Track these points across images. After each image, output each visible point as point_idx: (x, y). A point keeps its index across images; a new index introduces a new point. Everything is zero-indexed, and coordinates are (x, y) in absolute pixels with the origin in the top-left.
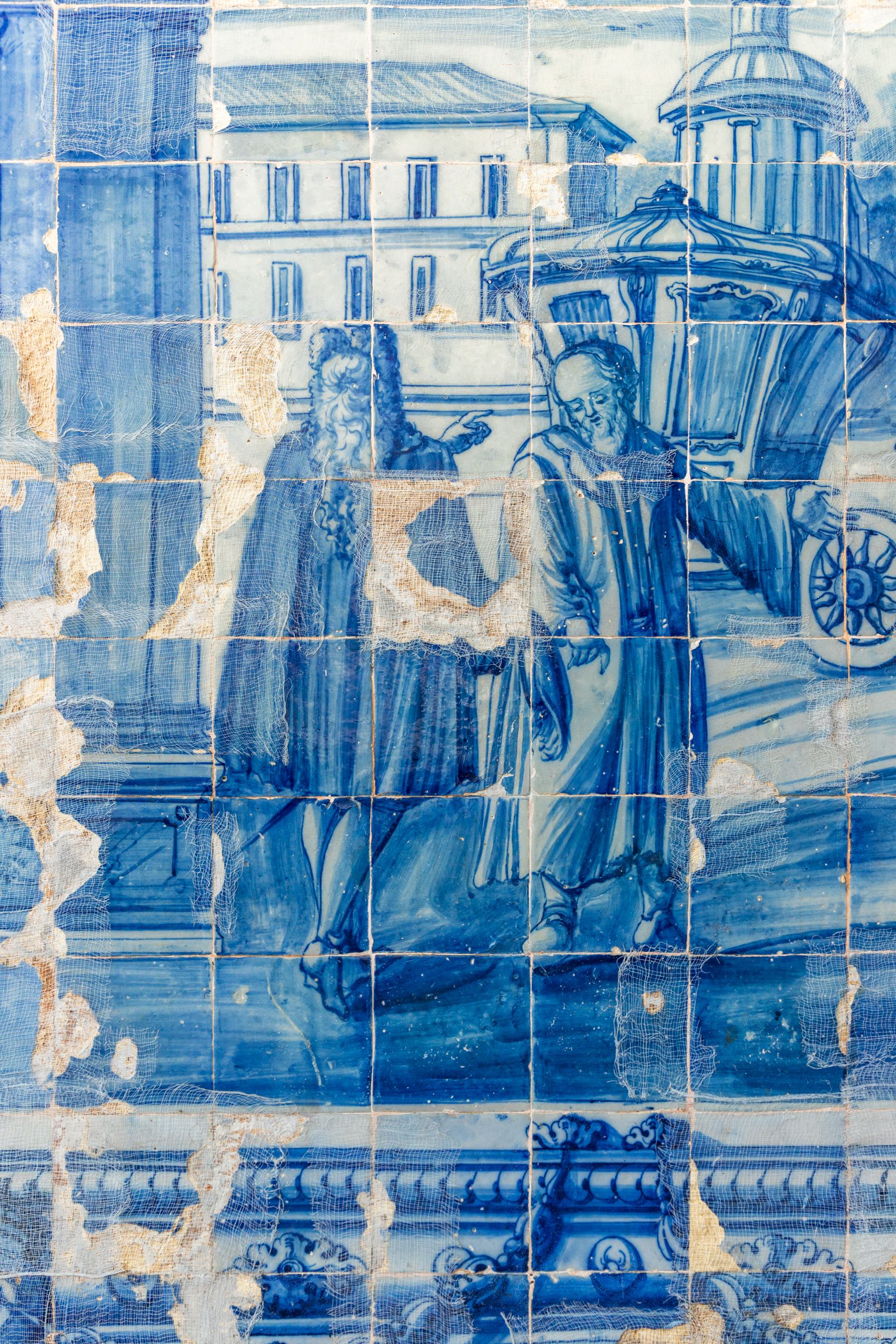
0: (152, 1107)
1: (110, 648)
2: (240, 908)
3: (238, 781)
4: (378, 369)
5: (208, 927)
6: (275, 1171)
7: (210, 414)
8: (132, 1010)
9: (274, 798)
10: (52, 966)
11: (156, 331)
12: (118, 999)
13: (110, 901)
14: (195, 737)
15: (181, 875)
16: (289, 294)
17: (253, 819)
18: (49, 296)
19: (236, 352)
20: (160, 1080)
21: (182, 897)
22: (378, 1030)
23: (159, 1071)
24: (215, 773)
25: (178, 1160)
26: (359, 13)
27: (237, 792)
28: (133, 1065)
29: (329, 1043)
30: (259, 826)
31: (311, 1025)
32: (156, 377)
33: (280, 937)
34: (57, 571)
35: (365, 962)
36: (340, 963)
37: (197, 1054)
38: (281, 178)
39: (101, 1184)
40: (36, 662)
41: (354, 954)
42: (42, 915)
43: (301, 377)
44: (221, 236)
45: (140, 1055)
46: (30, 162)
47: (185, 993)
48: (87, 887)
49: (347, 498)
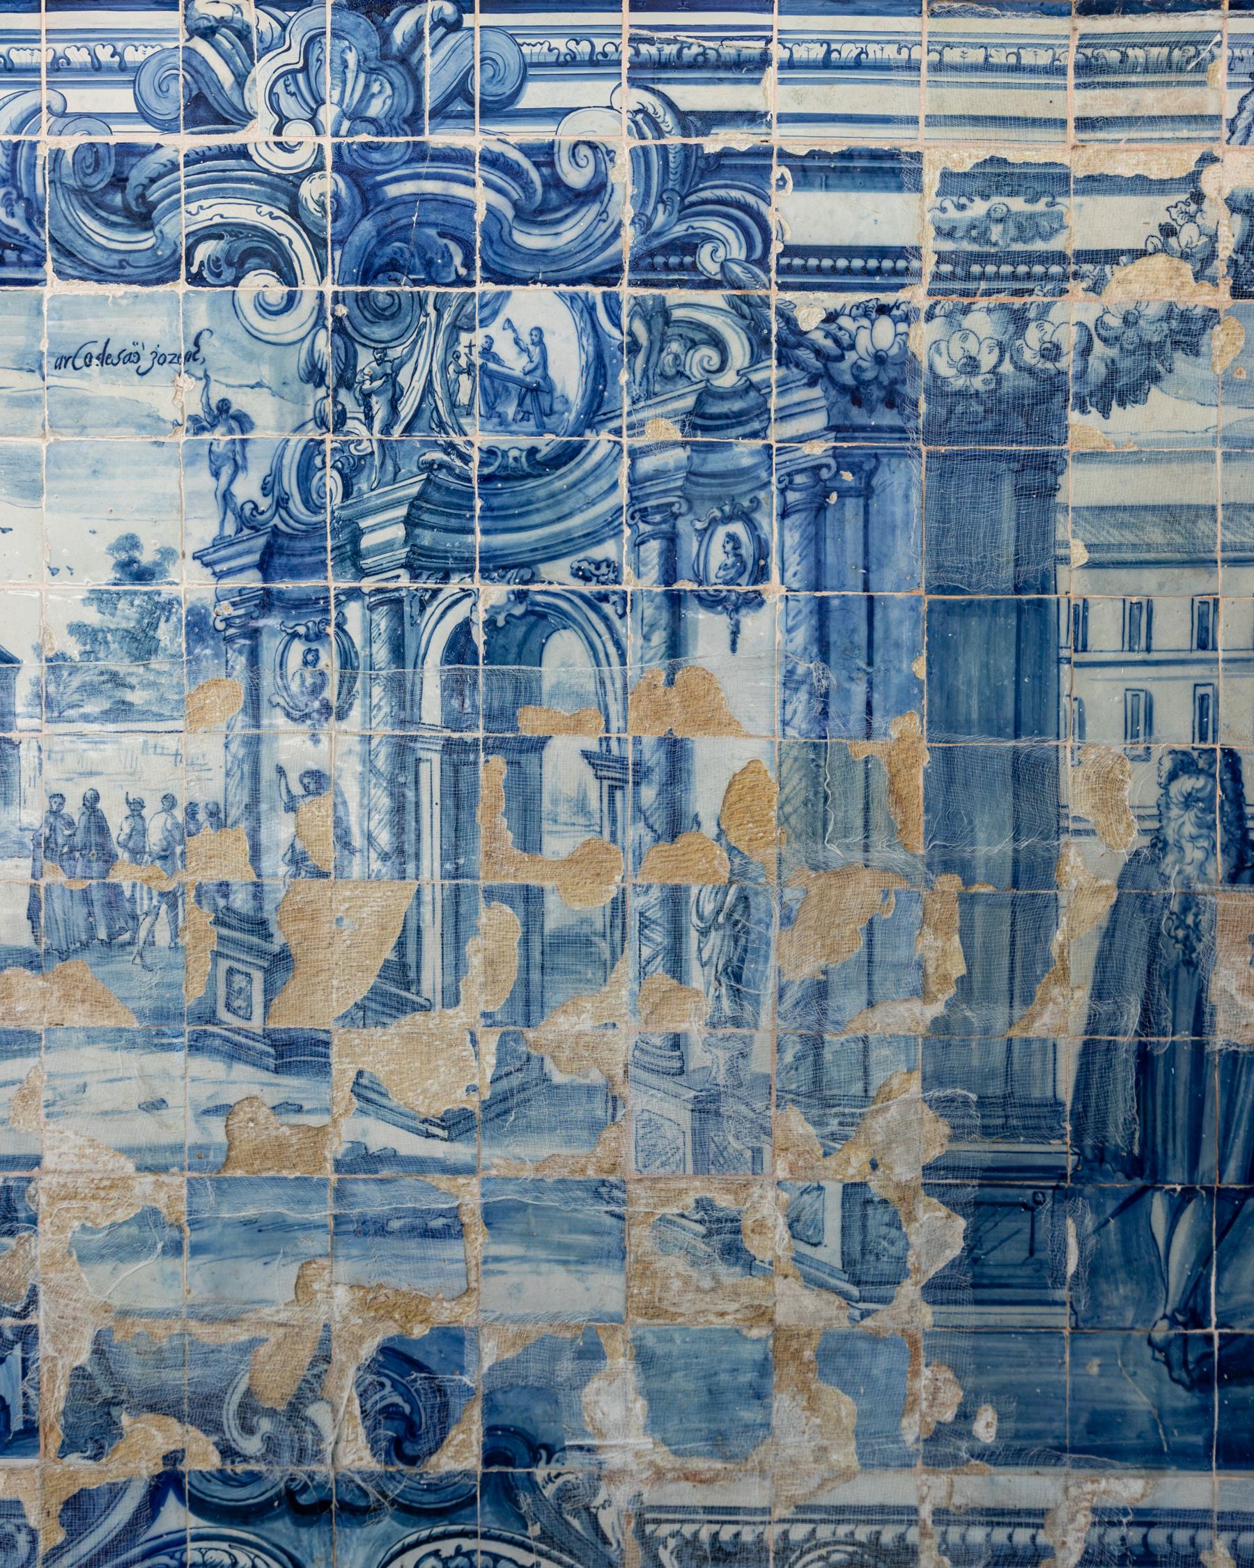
0: (1012, 1469)
1: (974, 1045)
2: (1092, 1285)
3: (1092, 1169)
4: (1223, 790)
5: (1063, 1304)
6: (1124, 1530)
7: (1067, 830)
8: (992, 1379)
9: (1123, 1185)
10: (919, 1336)
11: (1016, 752)
12: (980, 1369)
13: (970, 1280)
14: (1052, 1129)
15: (1038, 1255)
16: (1140, 718)
17: (1103, 1205)
18: (917, 719)
19: (1090, 771)
20: (1017, 1444)
21: (1039, 1275)
22: (1221, 1401)
23: (1017, 1436)
24: (1070, 1161)
25: (1036, 1517)
26: (1209, 456)
27: (1090, 1180)
28: (993, 1431)
29: (1175, 1412)
30: (1109, 1211)
31: (1159, 1395)
32: (1016, 796)
33: (1130, 1315)
34: (925, 975)
35: (1209, 1339)
36: (1185, 1338)
37: (1051, 1420)
38: (1136, 612)
39: (963, 1538)
40: (903, 1058)
41: (1199, 1331)
42: (909, 1291)
43: (1152, 795)
44: (1079, 665)
45: (1000, 1420)
46: (899, 595)
47: (1041, 1364)
48: (953, 1264)
49: (1194, 910)
